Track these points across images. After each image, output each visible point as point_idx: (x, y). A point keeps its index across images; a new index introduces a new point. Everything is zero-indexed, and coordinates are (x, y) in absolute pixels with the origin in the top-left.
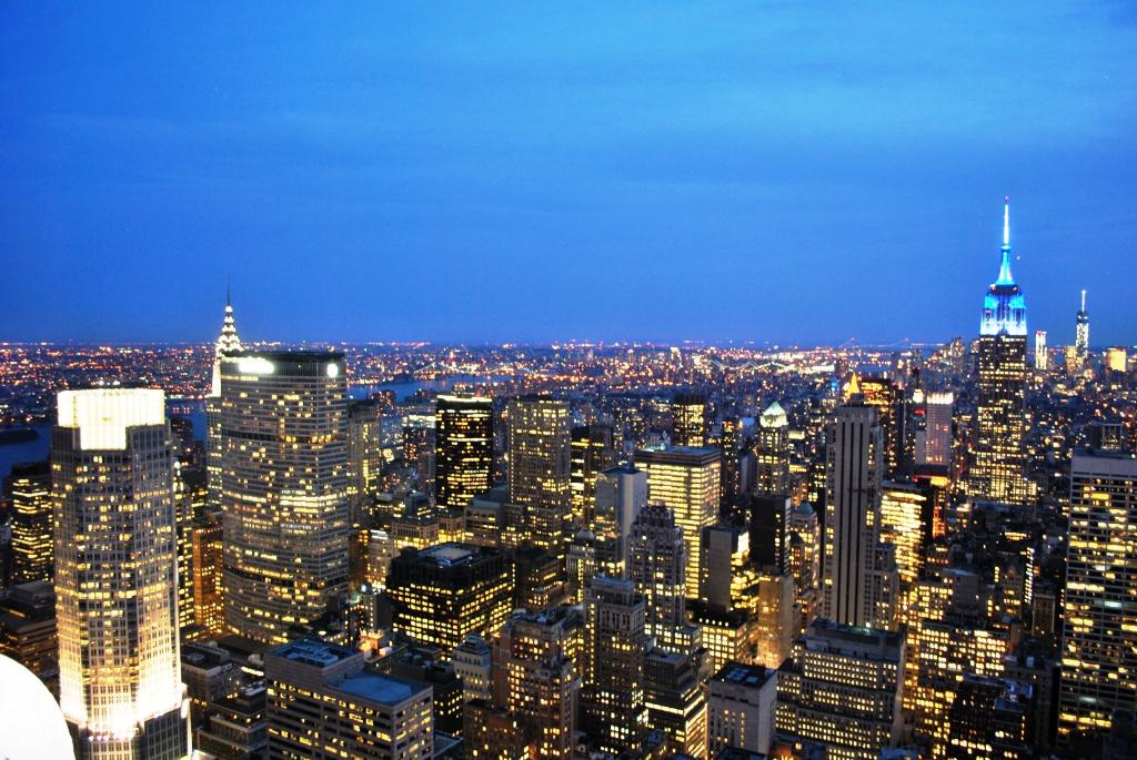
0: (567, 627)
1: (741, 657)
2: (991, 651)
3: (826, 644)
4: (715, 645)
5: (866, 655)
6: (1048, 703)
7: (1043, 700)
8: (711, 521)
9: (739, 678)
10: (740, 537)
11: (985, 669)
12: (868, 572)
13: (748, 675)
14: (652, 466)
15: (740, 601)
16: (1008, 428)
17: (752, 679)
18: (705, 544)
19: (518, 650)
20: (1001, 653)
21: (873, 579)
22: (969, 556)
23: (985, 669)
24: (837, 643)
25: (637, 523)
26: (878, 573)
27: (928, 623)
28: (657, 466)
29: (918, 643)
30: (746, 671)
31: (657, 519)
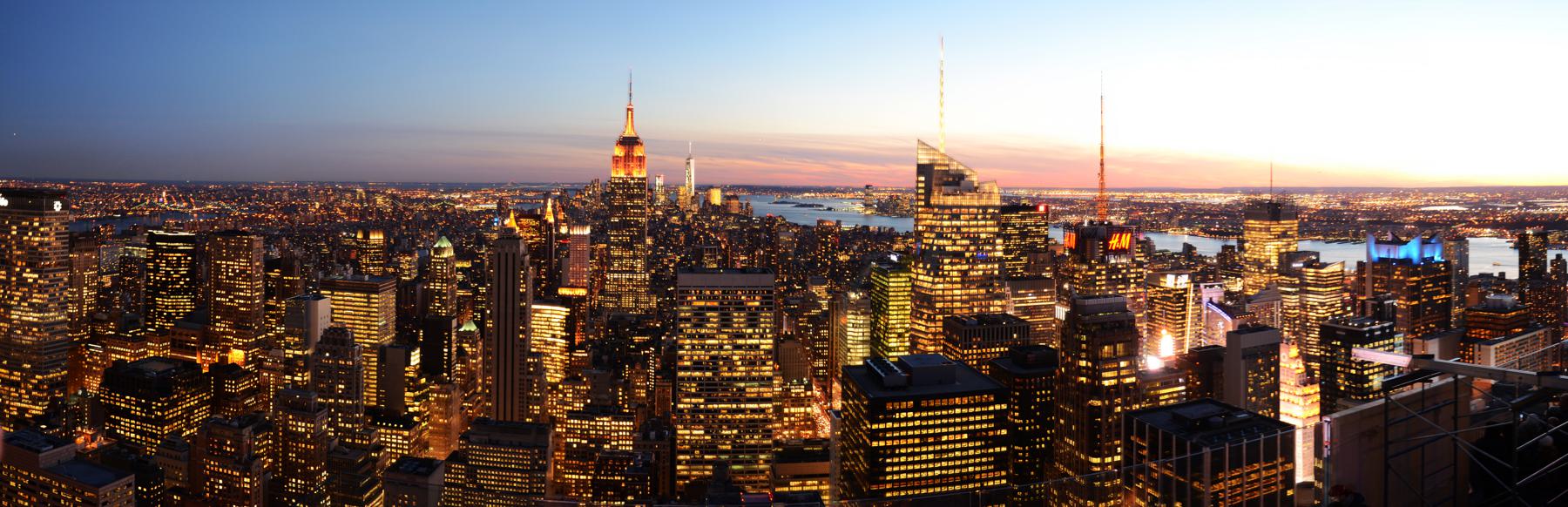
1: (415, 452)
2: (622, 431)
3: (486, 438)
7: (664, 462)
8: (387, 339)
9: (410, 469)
10: (413, 353)
12: (522, 377)
14: (335, 293)
15: (413, 406)
16: (634, 253)
18: (382, 359)
20: (629, 431)
21: (525, 382)
22: (605, 358)
25: (321, 342)
26: (530, 377)
27: (572, 415)
28: (340, 293)
29: (564, 430)
30: (417, 463)
31: (338, 339)
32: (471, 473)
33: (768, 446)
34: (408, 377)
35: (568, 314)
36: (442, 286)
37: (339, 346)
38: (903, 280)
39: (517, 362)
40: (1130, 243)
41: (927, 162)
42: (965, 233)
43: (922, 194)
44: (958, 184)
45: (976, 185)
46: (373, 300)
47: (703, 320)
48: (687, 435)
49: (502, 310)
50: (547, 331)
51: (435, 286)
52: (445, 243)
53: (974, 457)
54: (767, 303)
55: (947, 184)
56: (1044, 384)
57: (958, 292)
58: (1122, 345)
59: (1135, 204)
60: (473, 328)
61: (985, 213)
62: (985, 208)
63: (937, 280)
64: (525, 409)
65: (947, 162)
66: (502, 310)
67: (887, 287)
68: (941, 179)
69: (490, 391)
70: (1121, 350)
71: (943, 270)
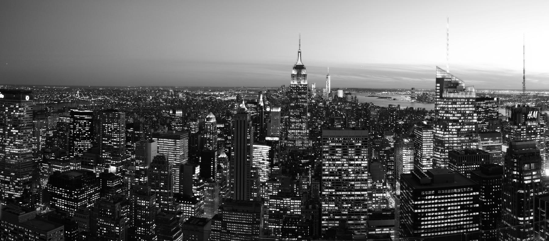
0: (122, 205)
1: (197, 215)
3: (232, 208)
5: (247, 211)
8: (184, 161)
10: (196, 168)
13: (199, 222)
14: (159, 139)
15: (196, 193)
18: (181, 171)
22: (288, 170)
25: (152, 163)
27: (272, 197)
28: (162, 139)
29: (268, 204)
30: (198, 220)
31: (161, 161)
32: (224, 225)
33: (365, 212)
34: (194, 179)
35: (270, 149)
36: (210, 136)
37: (161, 164)
38: (430, 133)
40: (537, 116)
42: (459, 111)
43: (438, 92)
44: (456, 87)
45: (464, 88)
46: (178, 143)
47: (334, 152)
48: (327, 207)
49: (239, 148)
50: (260, 157)
51: (207, 136)
52: (212, 116)
54: (364, 144)
55: (450, 87)
56: (496, 183)
58: (533, 164)
59: (540, 97)
60: (225, 156)
61: (468, 101)
62: (468, 99)
63: (445, 133)
64: (250, 194)
65: (450, 77)
66: (239, 148)
67: (422, 137)
68: (447, 85)
69: (233, 186)
70: (533, 166)
71: (448, 128)
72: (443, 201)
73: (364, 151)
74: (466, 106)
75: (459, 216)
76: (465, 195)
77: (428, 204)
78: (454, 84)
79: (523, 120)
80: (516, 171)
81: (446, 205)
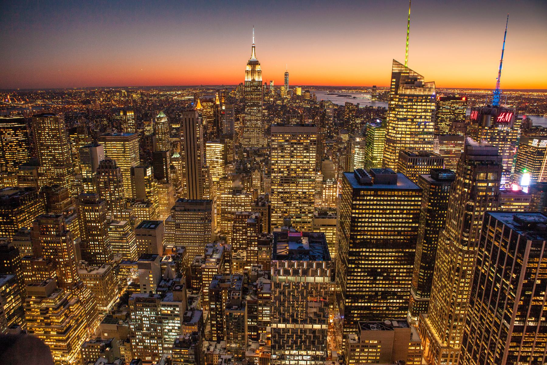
4: (141, 215)
6: (267, 218)
8: (135, 164)
11: (245, 209)
12: (200, 178)
17: (153, 226)
18: (133, 173)
19: (43, 231)
23: (245, 209)
24: (188, 207)
26: (203, 178)
39: (197, 171)
41: (397, 71)
43: (393, 88)
45: (423, 84)
53: (402, 223)
57: (409, 139)
60: (178, 156)
61: (426, 99)
65: (408, 71)
68: (404, 80)
72: (382, 203)
73: (313, 148)
74: (423, 104)
75: (397, 220)
76: (406, 199)
77: (366, 205)
78: (411, 79)
79: (490, 123)
80: (468, 179)
81: (385, 207)
